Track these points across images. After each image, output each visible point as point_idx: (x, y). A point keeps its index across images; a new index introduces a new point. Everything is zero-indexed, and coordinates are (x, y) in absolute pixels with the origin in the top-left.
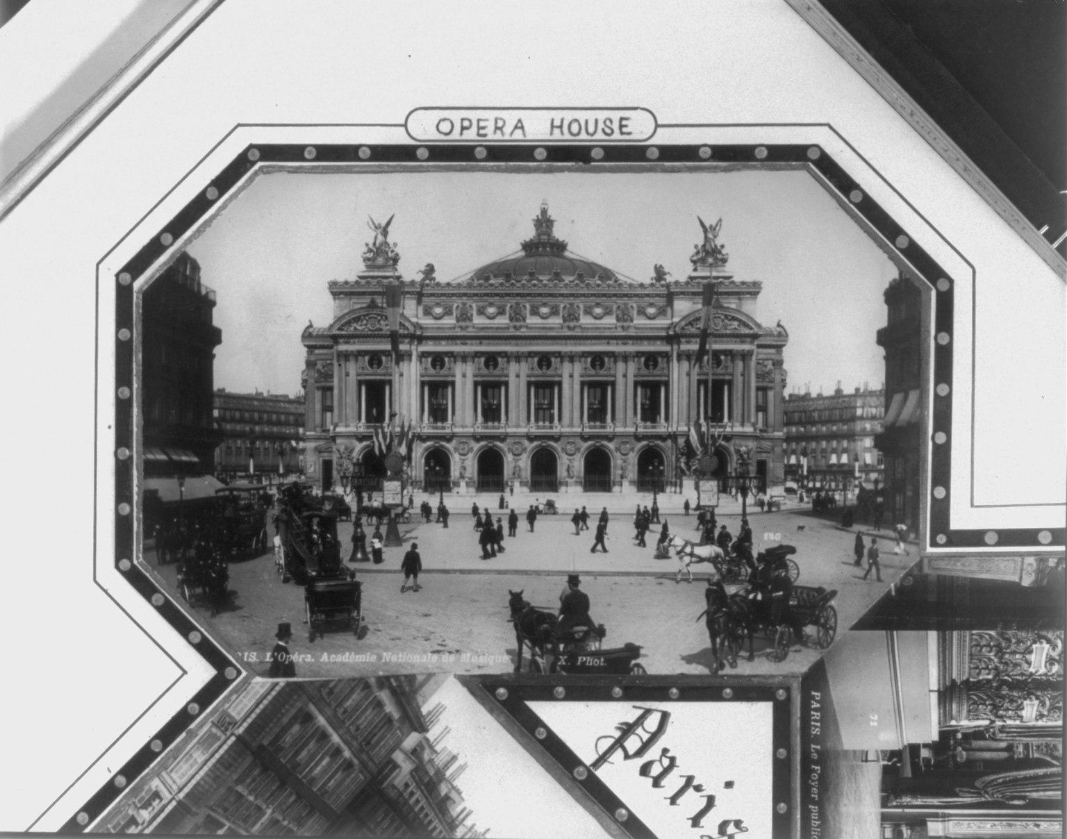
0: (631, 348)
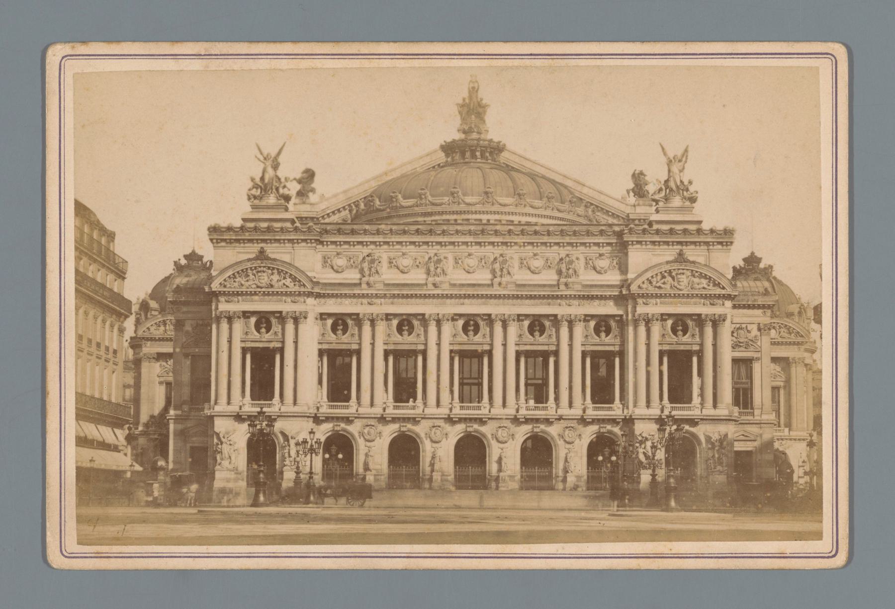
0: (577, 309)
